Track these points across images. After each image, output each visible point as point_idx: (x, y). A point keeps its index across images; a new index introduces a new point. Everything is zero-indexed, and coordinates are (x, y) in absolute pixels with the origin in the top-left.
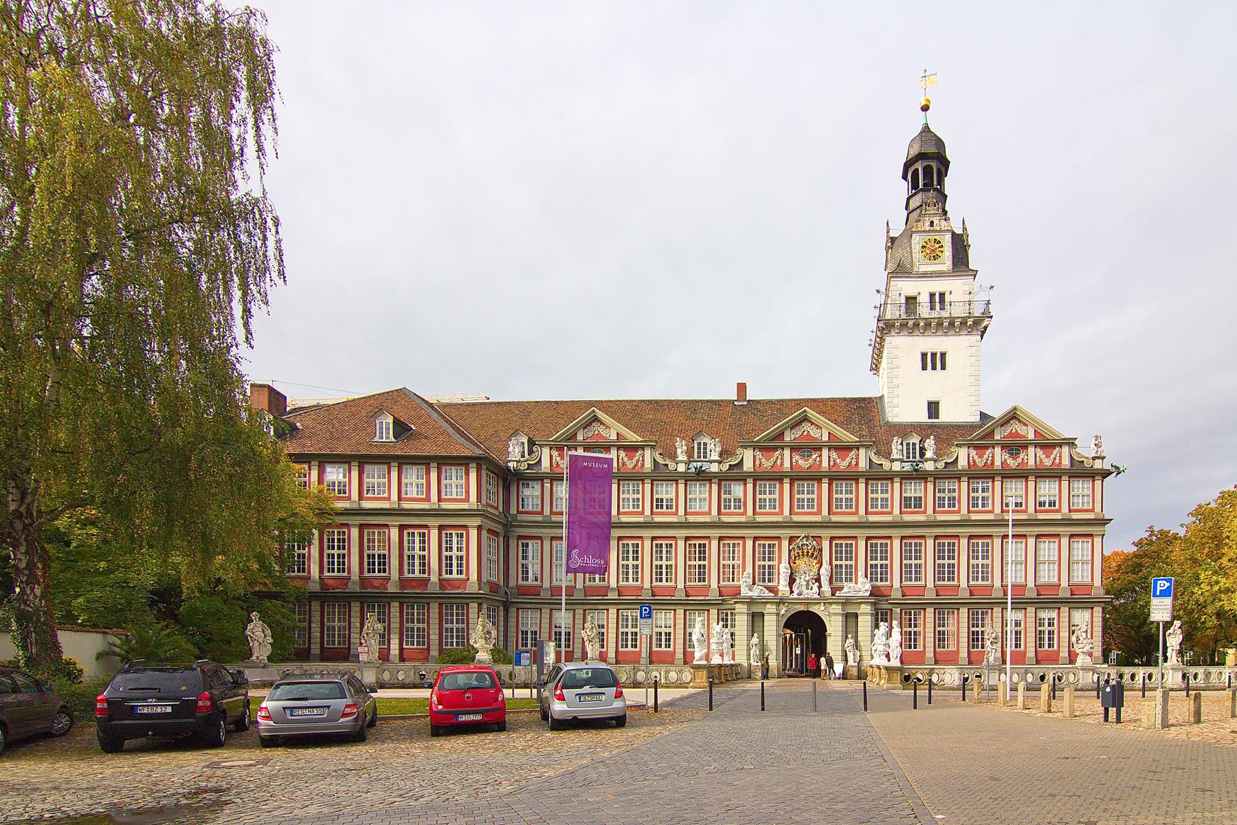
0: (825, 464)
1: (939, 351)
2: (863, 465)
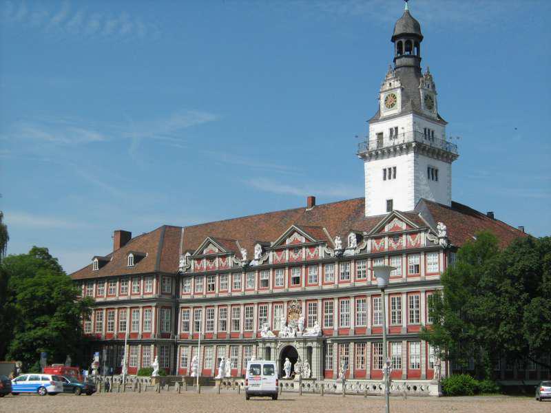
0: (304, 257)
1: (391, 166)
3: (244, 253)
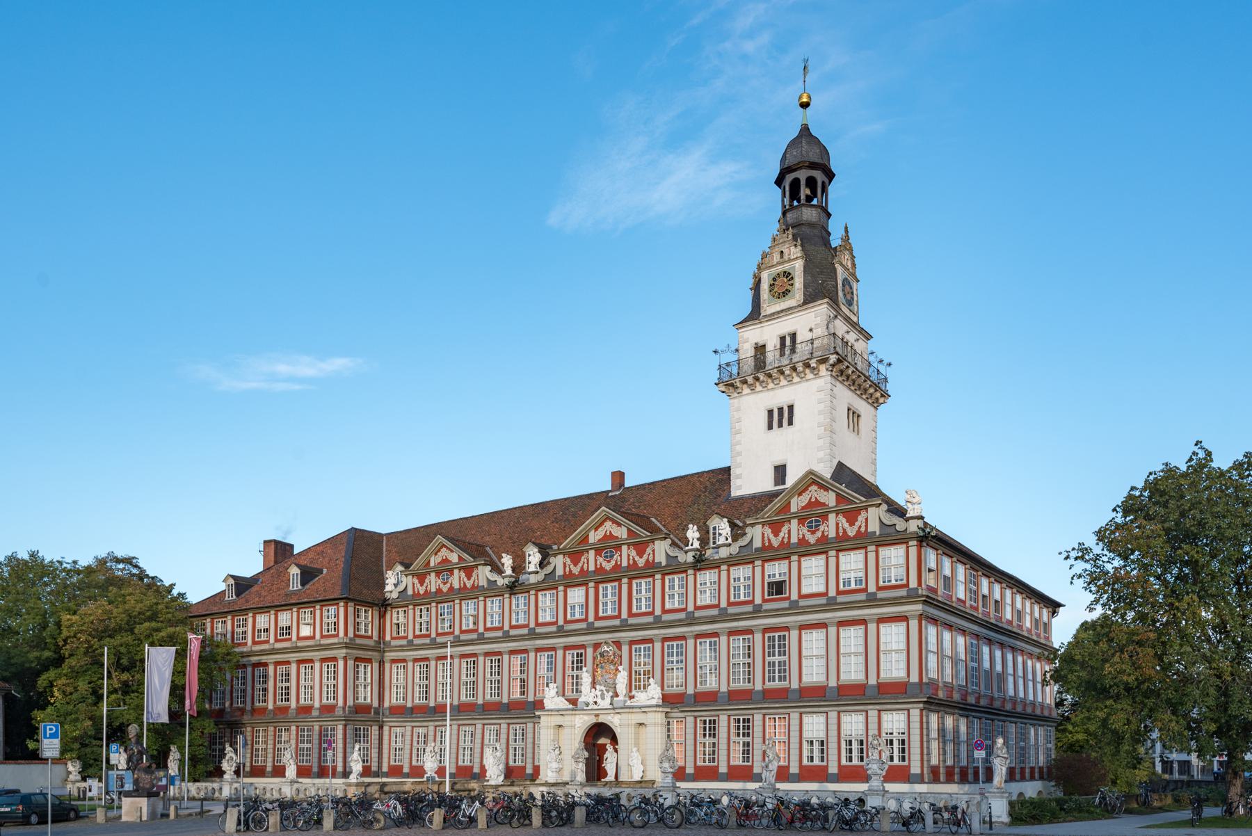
0: (625, 564)
2: (661, 558)
3: (507, 561)
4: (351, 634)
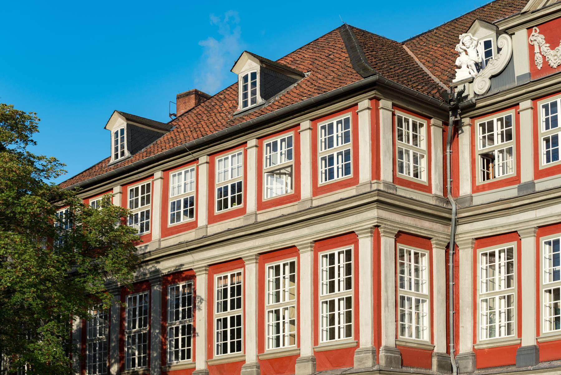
4: (386, 174)
